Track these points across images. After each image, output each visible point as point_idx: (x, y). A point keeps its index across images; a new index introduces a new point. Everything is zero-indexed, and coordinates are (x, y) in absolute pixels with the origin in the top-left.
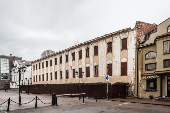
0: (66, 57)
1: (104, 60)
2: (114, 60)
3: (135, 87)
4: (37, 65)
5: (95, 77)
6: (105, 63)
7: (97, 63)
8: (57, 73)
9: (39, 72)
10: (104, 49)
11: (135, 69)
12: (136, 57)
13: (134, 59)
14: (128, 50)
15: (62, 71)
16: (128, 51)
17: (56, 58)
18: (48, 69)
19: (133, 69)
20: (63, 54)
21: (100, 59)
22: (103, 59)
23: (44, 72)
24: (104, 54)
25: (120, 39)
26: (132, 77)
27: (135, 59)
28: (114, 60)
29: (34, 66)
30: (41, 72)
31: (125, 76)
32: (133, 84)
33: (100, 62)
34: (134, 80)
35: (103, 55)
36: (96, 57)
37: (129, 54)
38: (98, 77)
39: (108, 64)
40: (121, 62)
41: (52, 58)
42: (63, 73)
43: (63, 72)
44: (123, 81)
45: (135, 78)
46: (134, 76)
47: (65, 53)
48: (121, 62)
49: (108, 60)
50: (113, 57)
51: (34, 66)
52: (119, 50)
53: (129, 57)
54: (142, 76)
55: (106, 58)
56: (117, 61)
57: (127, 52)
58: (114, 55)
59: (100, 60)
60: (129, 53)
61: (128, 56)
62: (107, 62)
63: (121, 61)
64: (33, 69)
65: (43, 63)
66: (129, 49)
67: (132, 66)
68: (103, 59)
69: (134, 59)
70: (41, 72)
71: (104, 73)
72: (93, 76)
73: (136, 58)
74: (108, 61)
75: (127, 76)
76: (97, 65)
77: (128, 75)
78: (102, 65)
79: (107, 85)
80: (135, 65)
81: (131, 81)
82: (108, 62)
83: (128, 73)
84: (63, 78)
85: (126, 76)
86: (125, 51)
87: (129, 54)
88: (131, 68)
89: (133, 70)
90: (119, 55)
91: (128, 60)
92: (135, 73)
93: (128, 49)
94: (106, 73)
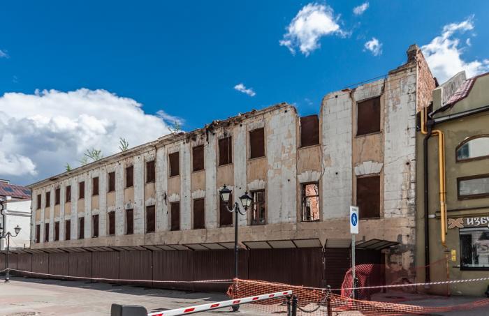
2: (327, 169)
3: (414, 257)
4: (48, 195)
5: (252, 224)
8: (116, 216)
11: (413, 194)
12: (416, 157)
13: (408, 164)
14: (386, 134)
15: (132, 210)
16: (383, 137)
18: (86, 204)
19: (405, 196)
26: (402, 224)
27: (413, 164)
28: (329, 171)
29: (39, 197)
31: (373, 220)
32: (409, 245)
36: (257, 161)
37: (389, 149)
38: (265, 224)
42: (136, 214)
43: (135, 212)
46: (413, 218)
48: (357, 176)
50: (324, 162)
51: (39, 197)
52: (350, 137)
54: (449, 217)
56: (340, 171)
57: (382, 141)
58: (326, 152)
60: (387, 144)
61: (386, 156)
66: (389, 132)
67: (403, 187)
69: (408, 164)
71: (289, 213)
72: (246, 221)
77: (386, 215)
80: (416, 182)
83: (386, 211)
85: (377, 221)
87: (389, 149)
88: (400, 193)
89: (405, 201)
91: (386, 168)
92: (416, 210)
93: (386, 132)
94: (295, 212)
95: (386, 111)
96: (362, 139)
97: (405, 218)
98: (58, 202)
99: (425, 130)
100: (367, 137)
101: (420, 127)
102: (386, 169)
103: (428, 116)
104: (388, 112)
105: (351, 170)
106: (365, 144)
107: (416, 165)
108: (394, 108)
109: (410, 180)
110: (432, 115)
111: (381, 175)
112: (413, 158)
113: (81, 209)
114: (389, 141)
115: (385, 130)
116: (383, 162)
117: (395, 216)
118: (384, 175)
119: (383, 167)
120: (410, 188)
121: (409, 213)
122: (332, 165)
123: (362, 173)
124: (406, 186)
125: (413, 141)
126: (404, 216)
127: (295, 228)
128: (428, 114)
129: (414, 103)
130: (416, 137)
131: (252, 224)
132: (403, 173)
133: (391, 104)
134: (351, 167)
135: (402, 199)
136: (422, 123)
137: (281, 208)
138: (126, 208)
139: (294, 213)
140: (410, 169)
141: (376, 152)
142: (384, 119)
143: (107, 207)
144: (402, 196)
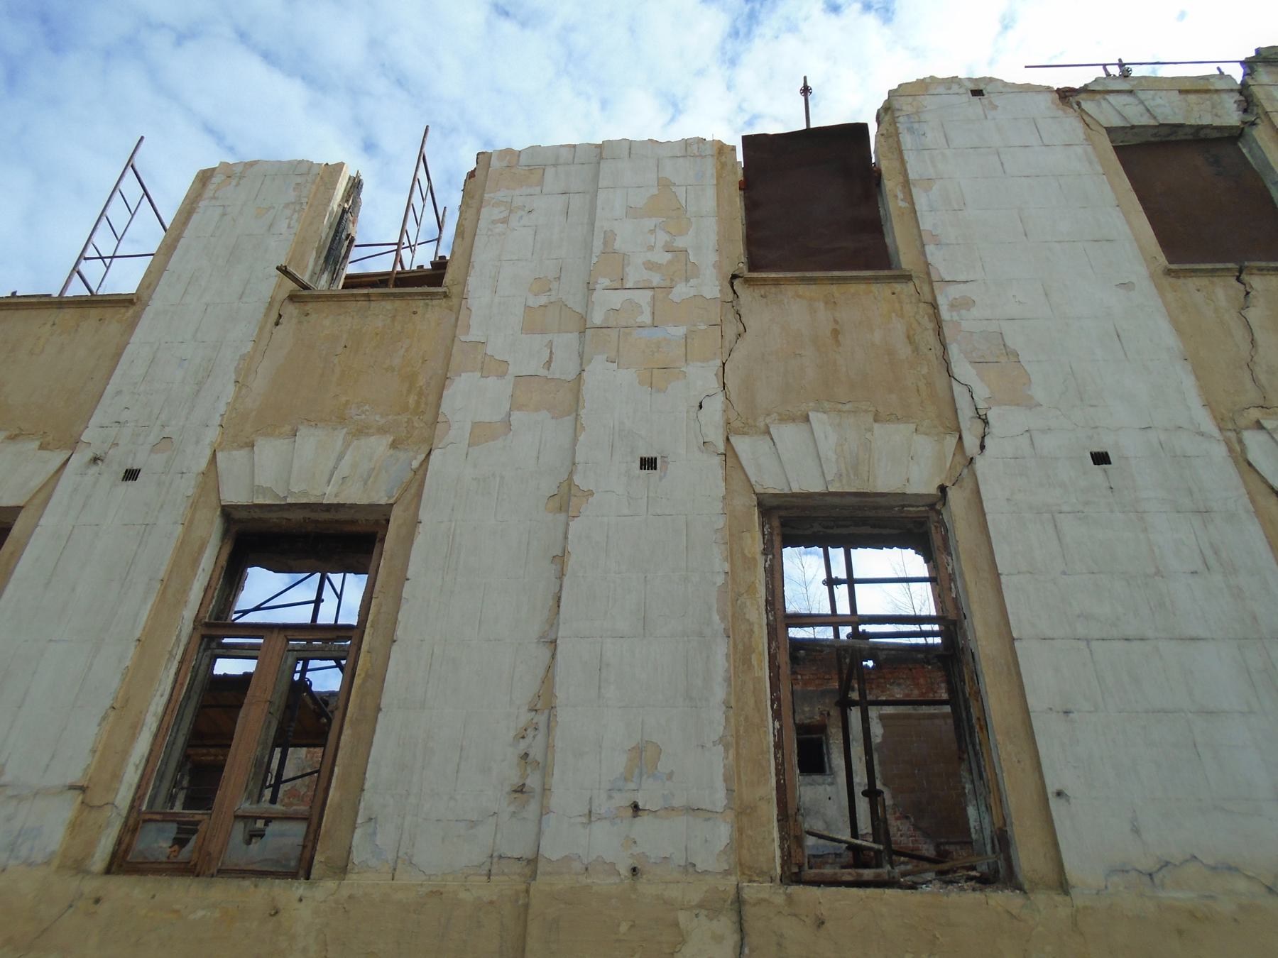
5: (121, 863)
7: (378, 446)
21: (492, 367)
22: (610, 384)
38: (302, 869)
55: (703, 377)
58: (965, 325)
59: (497, 389)
62: (740, 443)
71: (643, 757)
74: (788, 435)
78: (566, 499)
94: (717, 762)
106: (1253, 314)
131: (121, 863)
137: (544, 702)
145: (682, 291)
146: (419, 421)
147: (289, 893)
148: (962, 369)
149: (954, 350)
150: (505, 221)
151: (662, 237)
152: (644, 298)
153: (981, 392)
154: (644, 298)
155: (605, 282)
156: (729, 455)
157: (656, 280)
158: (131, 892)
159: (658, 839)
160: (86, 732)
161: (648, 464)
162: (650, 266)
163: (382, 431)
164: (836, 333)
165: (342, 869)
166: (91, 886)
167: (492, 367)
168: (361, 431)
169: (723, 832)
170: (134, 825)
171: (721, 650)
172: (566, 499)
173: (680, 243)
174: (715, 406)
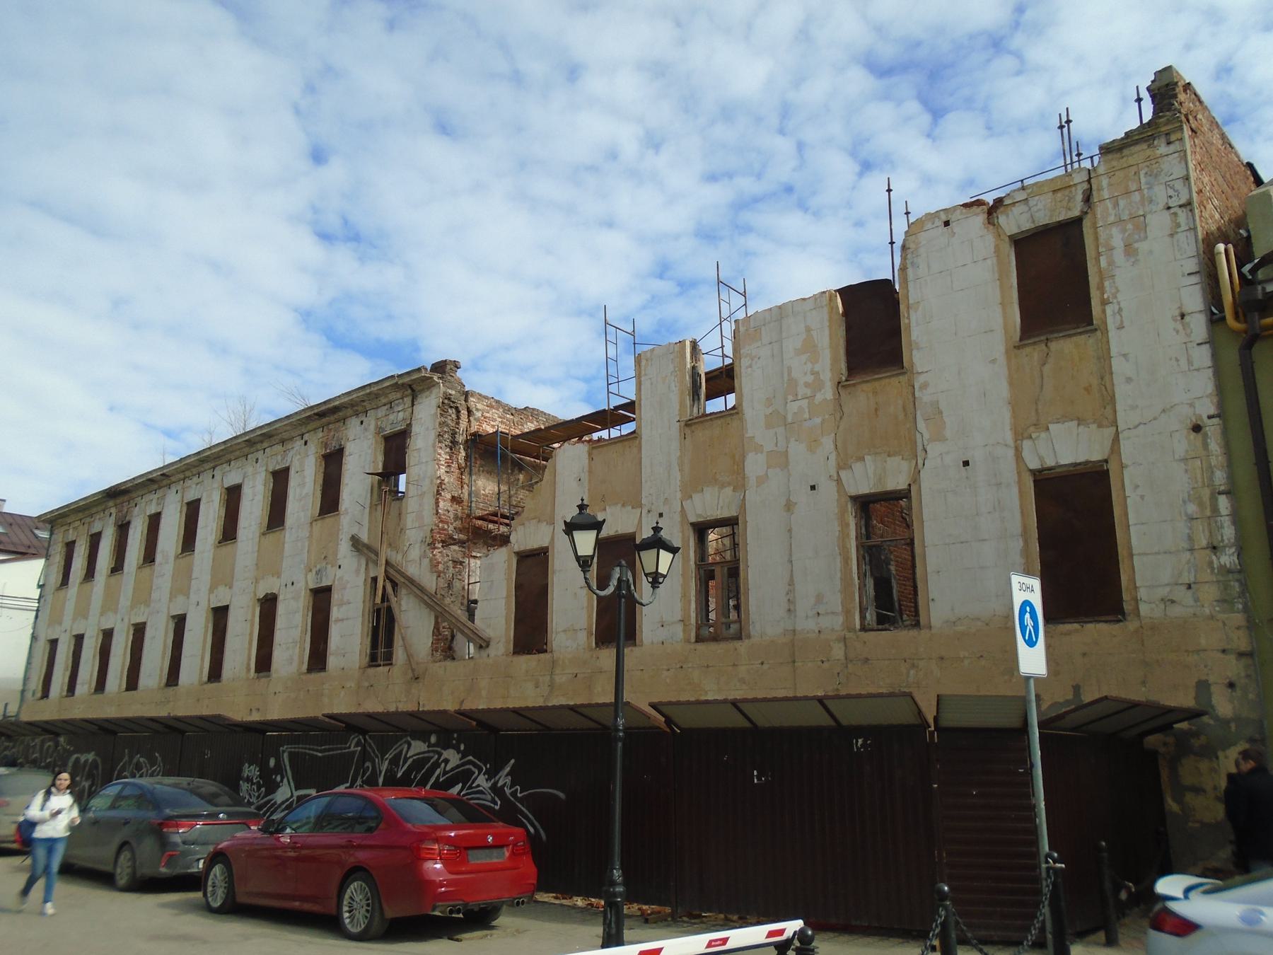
0: (387, 453)
1: (813, 461)
2: (934, 449)
5: (699, 639)
6: (828, 491)
7: (728, 491)
9: (110, 603)
10: (809, 348)
11: (1228, 532)
12: (1221, 404)
13: (1197, 428)
15: (328, 590)
17: (287, 470)
19: (1204, 543)
20: (354, 422)
21: (758, 449)
22: (797, 450)
23: (147, 602)
24: (802, 391)
25: (990, 239)
27: (1213, 428)
30: (125, 600)
33: (762, 480)
34: (1234, 668)
35: (793, 407)
37: (1129, 380)
38: (740, 638)
39: (865, 505)
40: (1034, 464)
41: (250, 470)
42: (341, 605)
43: (335, 596)
44: (1077, 689)
45: (1244, 645)
46: (1238, 618)
47: (382, 412)
48: (1034, 473)
49: (862, 459)
52: (998, 346)
53: (1134, 408)
55: (828, 443)
56: (976, 456)
57: (1104, 357)
58: (924, 397)
59: (761, 458)
60: (1117, 364)
62: (843, 474)
63: (1026, 454)
64: (56, 578)
65: (154, 522)
66: (1121, 327)
67: (1192, 508)
68: (797, 450)
69: (1197, 428)
70: (125, 600)
71: (819, 599)
72: (679, 629)
73: (1221, 414)
74: (857, 467)
75: (1131, 625)
76: (726, 514)
77: (1144, 609)
78: (789, 506)
79: (1024, 729)
81: (1203, 687)
82: (863, 480)
83: (1142, 593)
84: (332, 661)
85: (1116, 628)
86: (1067, 347)
90: (1003, 390)
92: (1244, 585)
95: (1103, 262)
96: (1033, 354)
97: (1212, 617)
98: (117, 567)
99: (1237, 317)
100: (1054, 346)
101: (1221, 310)
102: (1126, 448)
103: (1240, 274)
104: (1111, 263)
105: (1011, 452)
106: (1047, 366)
107: (1225, 432)
108: (1129, 250)
109: (1211, 484)
110: (1253, 271)
111: (1113, 467)
112: (1212, 411)
113: (182, 586)
114: (1125, 355)
115: (1110, 320)
116: (1115, 423)
117: (1175, 611)
118: (1122, 467)
119: (1116, 439)
120: (1215, 510)
121: (1225, 601)
122: (948, 433)
123: (1050, 462)
124: (1201, 505)
125: (1203, 356)
126: (1207, 611)
127: (838, 652)
128: (1239, 268)
129: (1191, 235)
130: (1211, 341)
131: (699, 639)
132: (1184, 460)
133: (1117, 240)
134: (1011, 442)
135: (1191, 550)
136: (1228, 298)
137: (791, 583)
138: (312, 586)
139: (835, 601)
140: (1205, 445)
141: (1088, 389)
142: (1101, 288)
143: (257, 581)
144: (1190, 538)
145: (819, 397)
146: (739, 482)
147: (737, 644)
148: (921, 425)
149: (918, 413)
150: (750, 366)
151: (809, 365)
152: (805, 403)
153: (926, 436)
154: (805, 403)
155: (790, 398)
156: (839, 481)
157: (809, 392)
158: (701, 647)
159: (825, 622)
160: (678, 606)
161: (813, 488)
162: (807, 385)
163: (729, 484)
164: (876, 410)
165: (749, 637)
166: (692, 646)
167: (758, 449)
168: (723, 486)
169: (841, 619)
170: (698, 628)
171: (839, 559)
172: (789, 506)
173: (817, 368)
174: (833, 457)
